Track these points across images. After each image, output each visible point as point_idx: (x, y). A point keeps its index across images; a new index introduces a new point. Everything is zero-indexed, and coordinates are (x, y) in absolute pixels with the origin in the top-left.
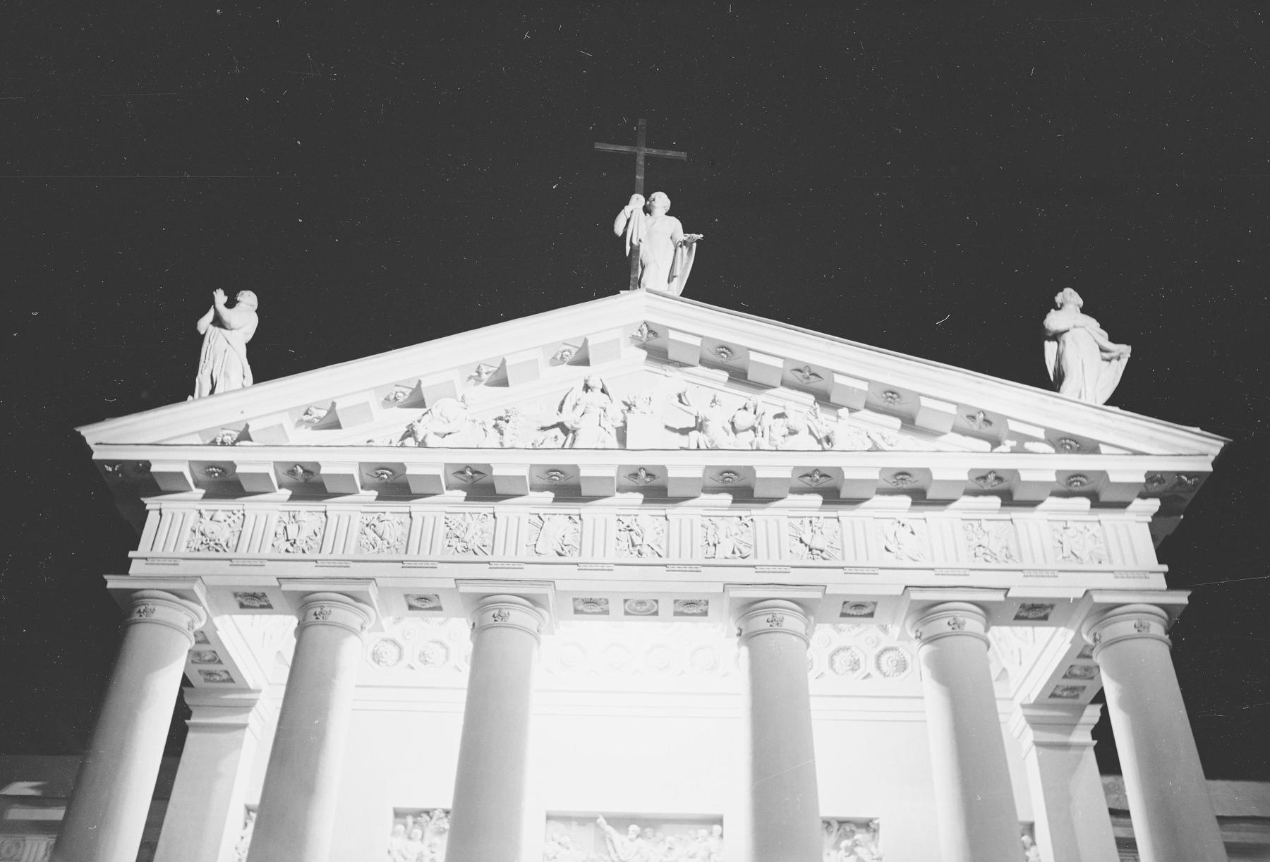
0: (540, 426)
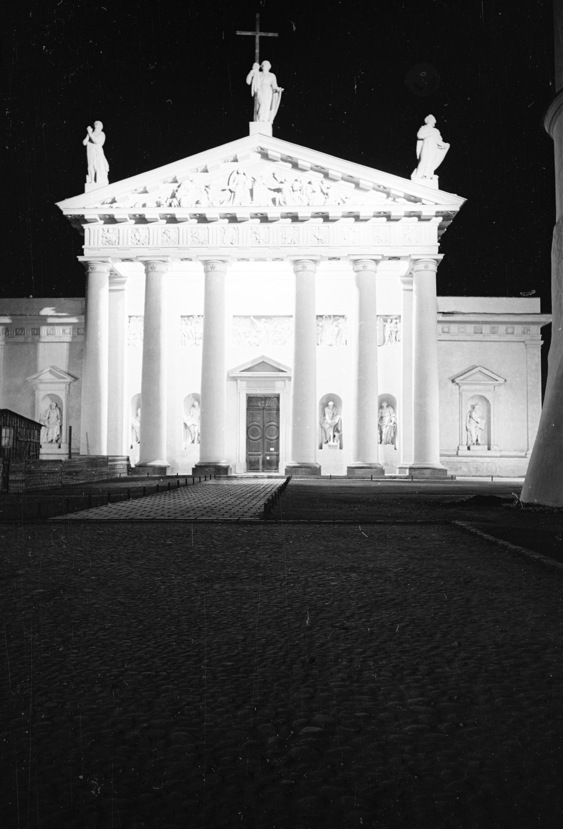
0: (222, 189)
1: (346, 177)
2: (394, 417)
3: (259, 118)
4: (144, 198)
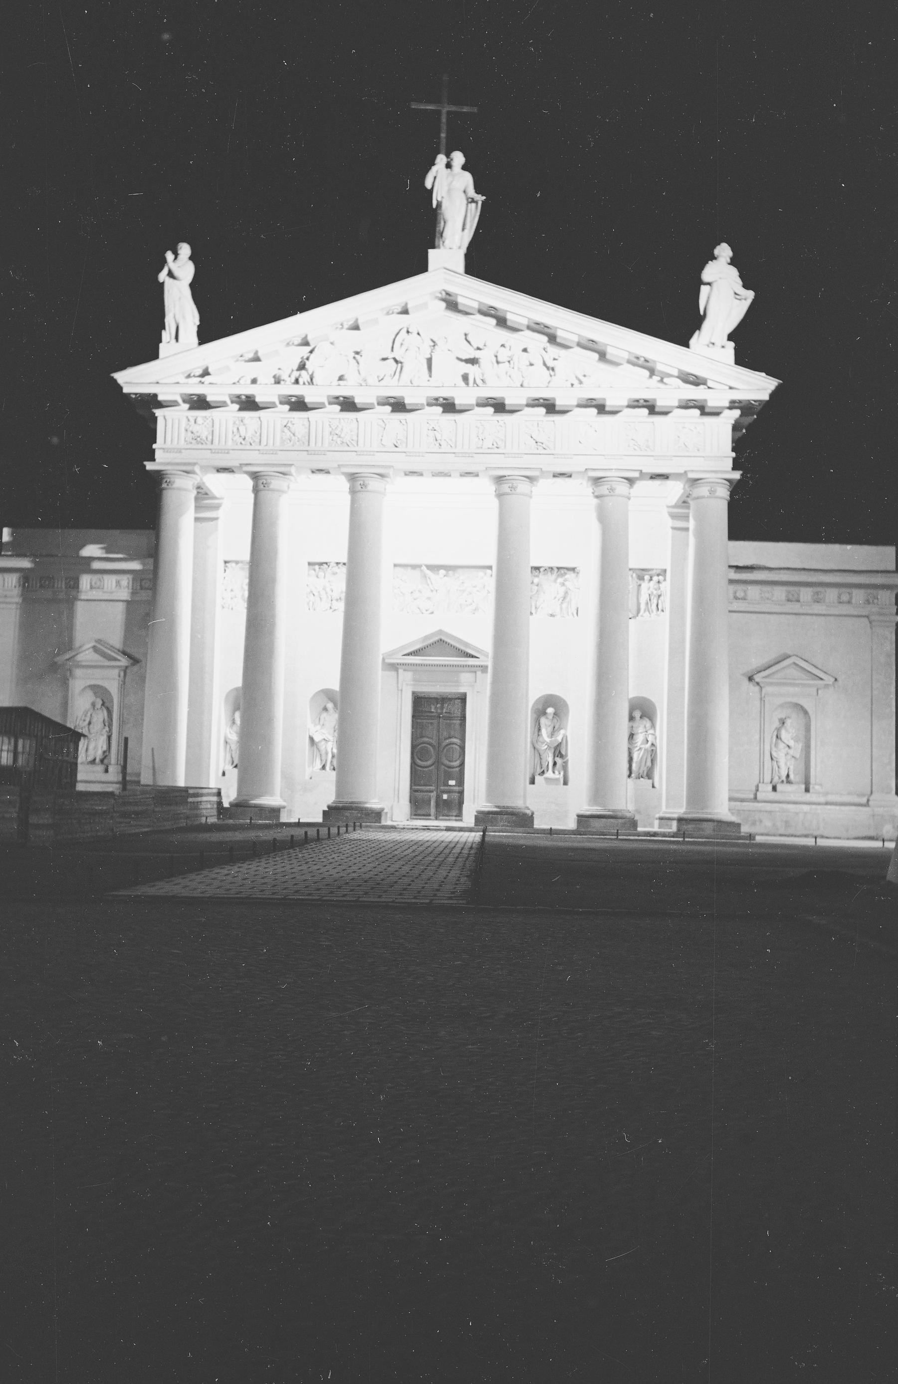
0: (381, 357)
1: (584, 342)
2: (652, 734)
3: (443, 242)
4: (254, 369)
